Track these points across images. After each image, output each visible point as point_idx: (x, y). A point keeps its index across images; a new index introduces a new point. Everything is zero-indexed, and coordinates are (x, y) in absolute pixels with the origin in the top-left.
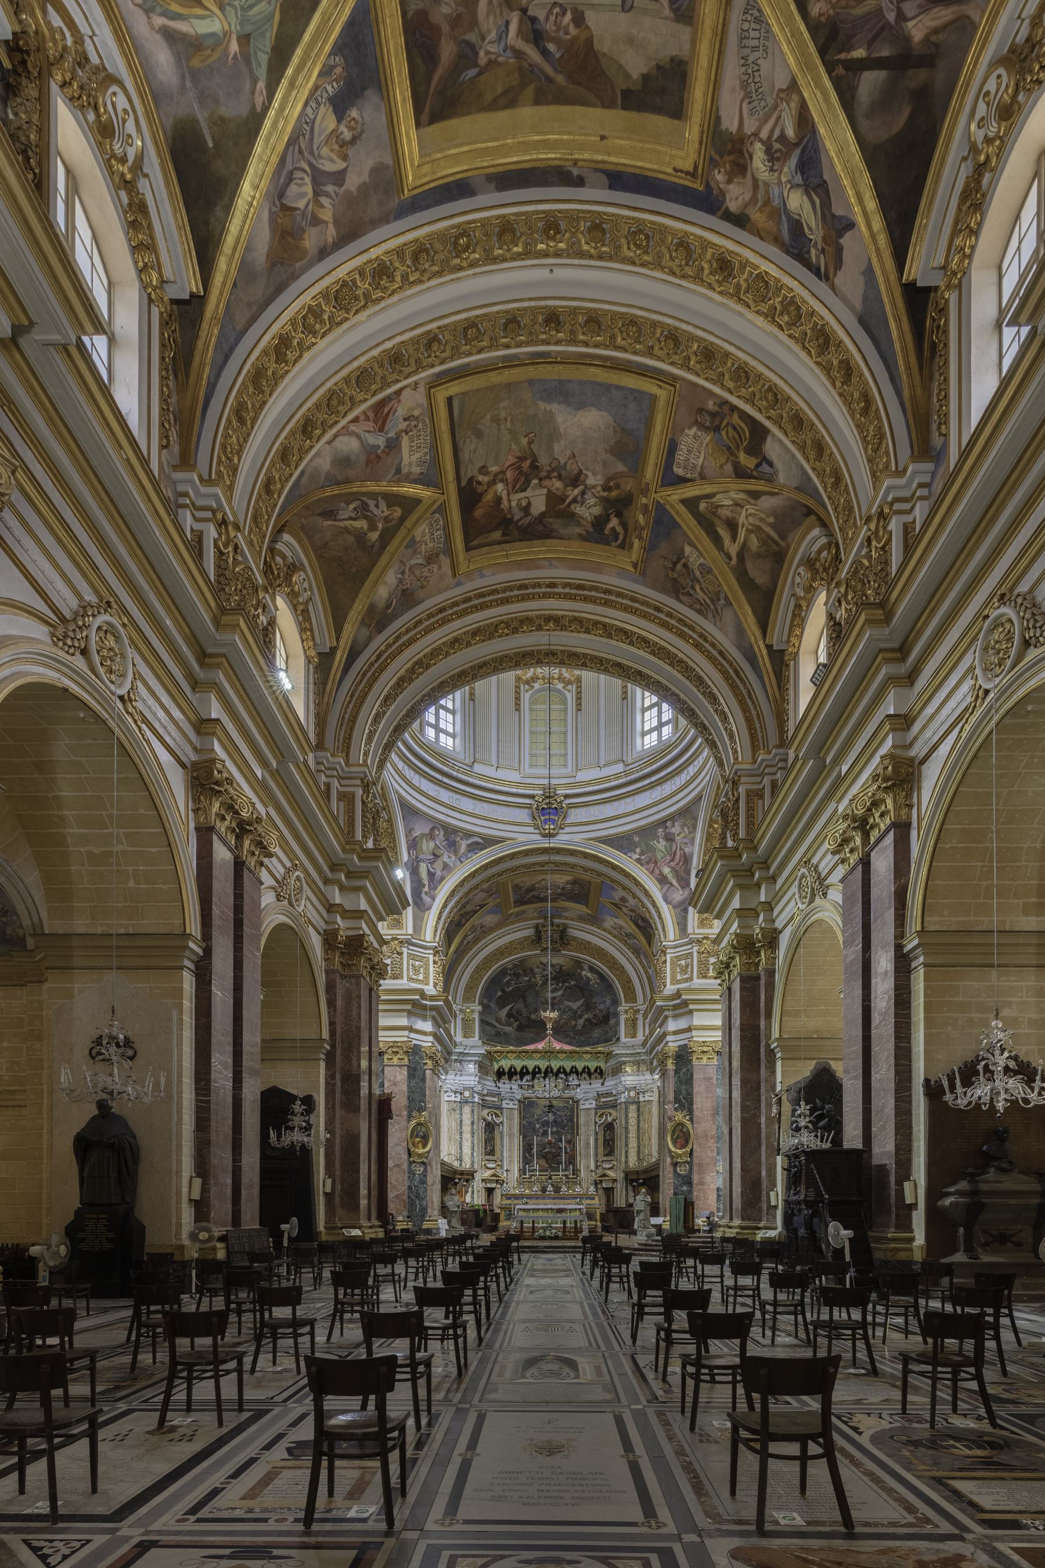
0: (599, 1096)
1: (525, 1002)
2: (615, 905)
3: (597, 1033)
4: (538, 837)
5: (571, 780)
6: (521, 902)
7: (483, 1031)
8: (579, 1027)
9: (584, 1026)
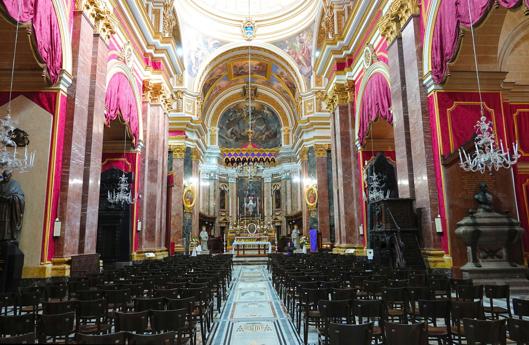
0: (273, 175)
1: (239, 126)
2: (278, 76)
3: (271, 142)
4: (245, 41)
5: (259, 14)
6: (237, 75)
7: (220, 141)
8: (263, 139)
9: (265, 139)
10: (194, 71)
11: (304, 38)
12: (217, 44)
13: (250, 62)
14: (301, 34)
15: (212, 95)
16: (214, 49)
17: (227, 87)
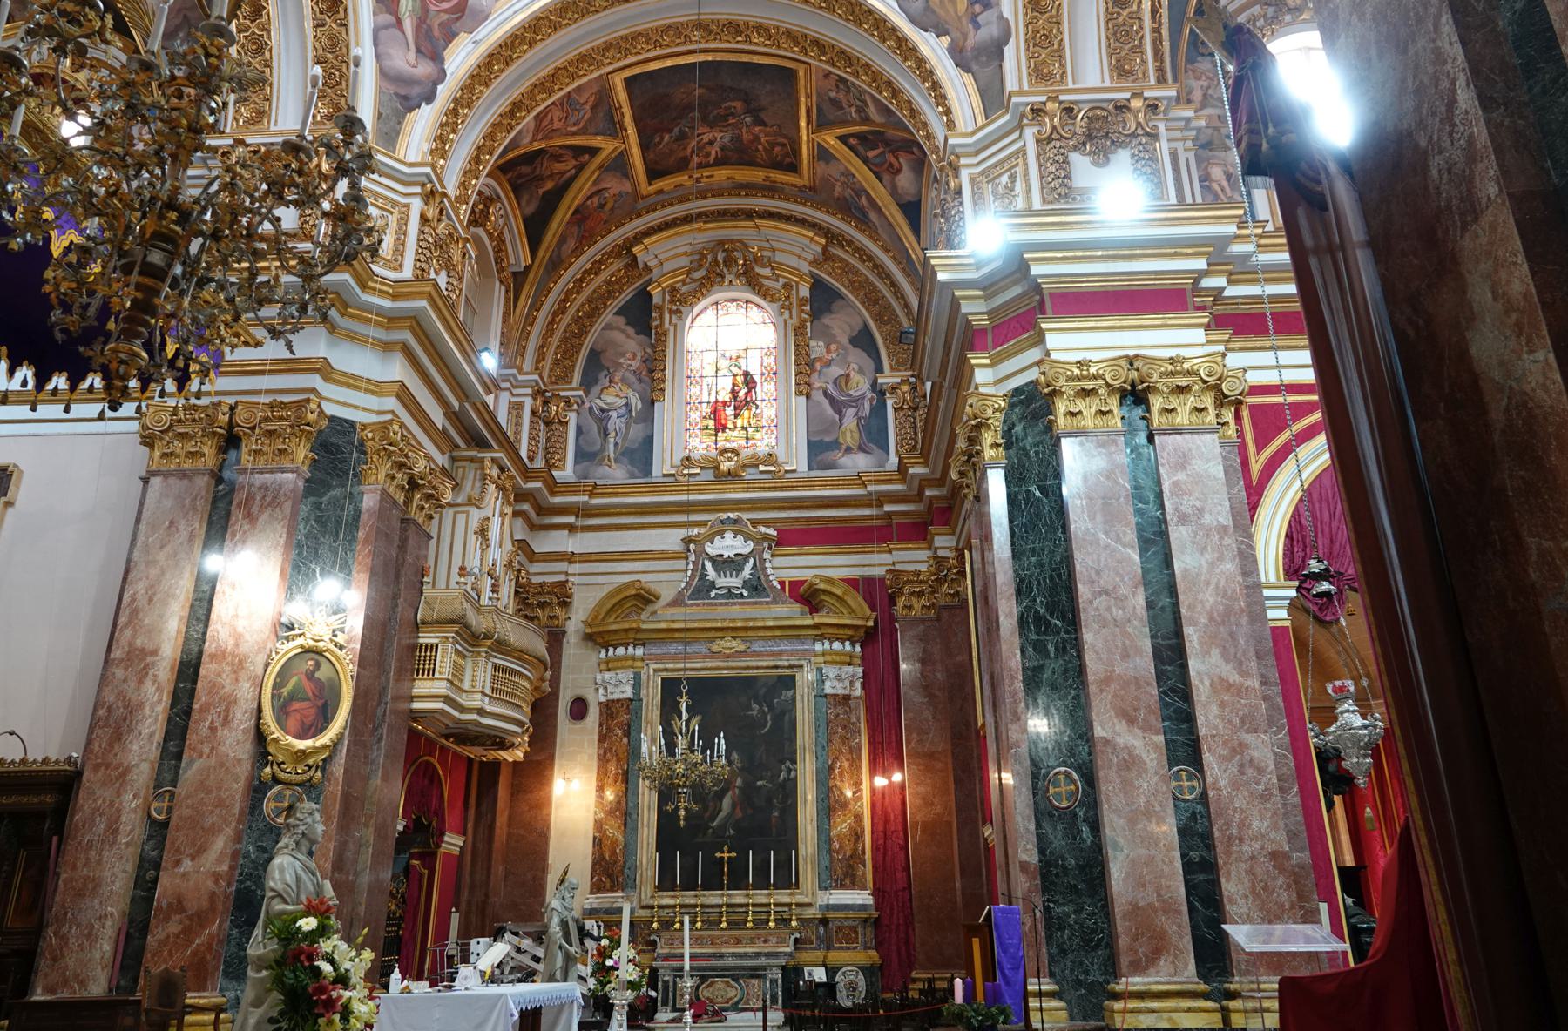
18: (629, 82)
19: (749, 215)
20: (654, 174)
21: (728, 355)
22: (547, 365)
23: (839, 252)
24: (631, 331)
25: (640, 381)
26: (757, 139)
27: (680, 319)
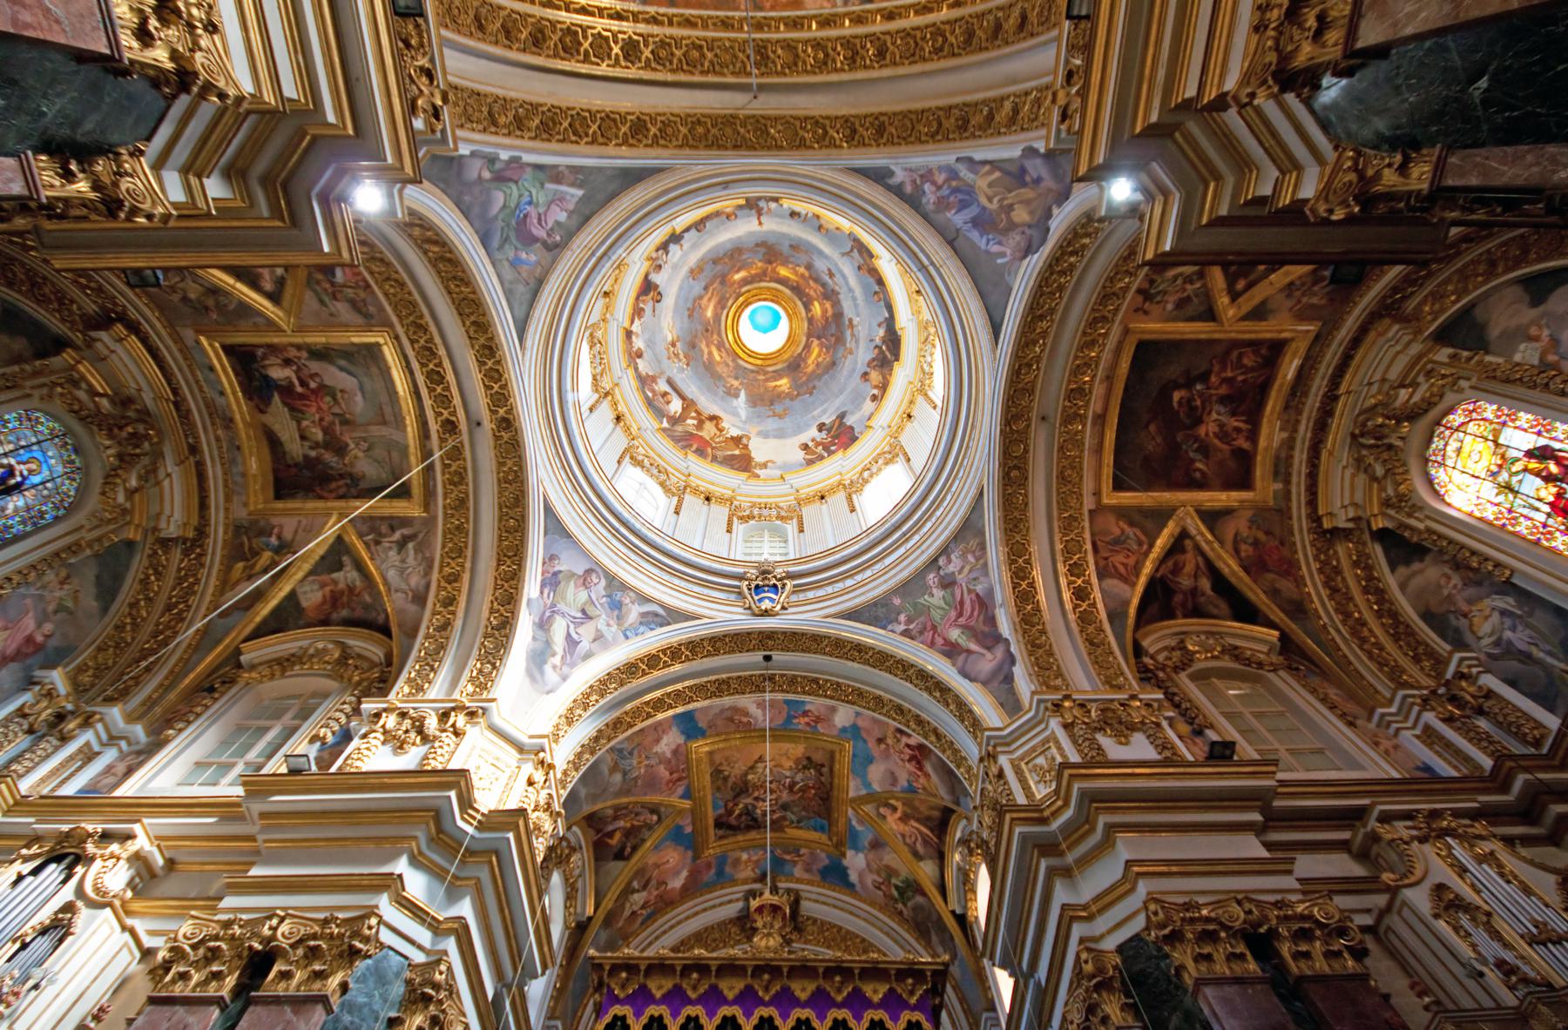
10: (551, 676)
11: (951, 568)
12: (656, 615)
13: (768, 749)
14: (941, 562)
15: (627, 913)
16: (642, 629)
17: (690, 891)
18: (1118, 486)
19: (1331, 398)
20: (1243, 480)
21: (1495, 469)
22: (1413, 672)
23: (1411, 305)
24: (1416, 566)
25: (1479, 584)
26: (1225, 380)
27: (1421, 508)
